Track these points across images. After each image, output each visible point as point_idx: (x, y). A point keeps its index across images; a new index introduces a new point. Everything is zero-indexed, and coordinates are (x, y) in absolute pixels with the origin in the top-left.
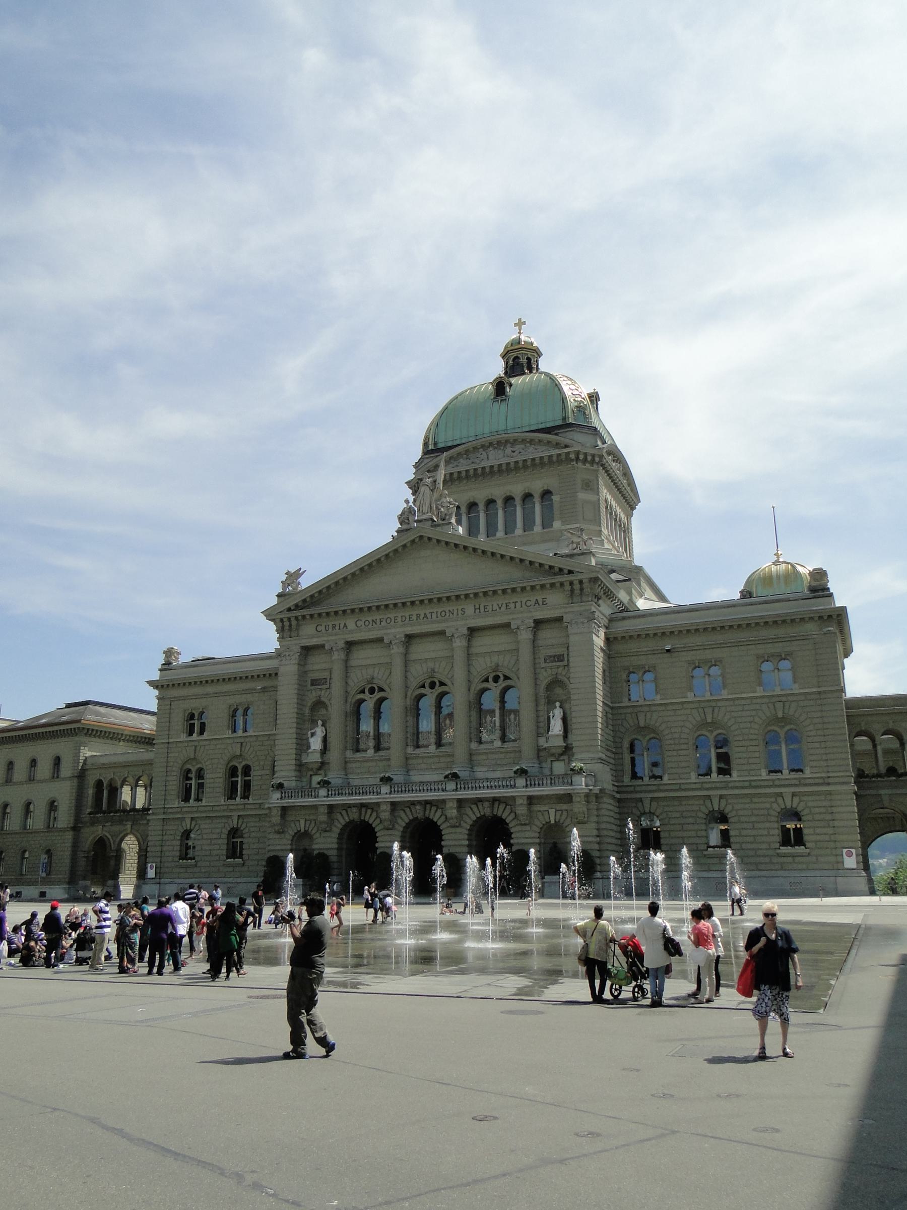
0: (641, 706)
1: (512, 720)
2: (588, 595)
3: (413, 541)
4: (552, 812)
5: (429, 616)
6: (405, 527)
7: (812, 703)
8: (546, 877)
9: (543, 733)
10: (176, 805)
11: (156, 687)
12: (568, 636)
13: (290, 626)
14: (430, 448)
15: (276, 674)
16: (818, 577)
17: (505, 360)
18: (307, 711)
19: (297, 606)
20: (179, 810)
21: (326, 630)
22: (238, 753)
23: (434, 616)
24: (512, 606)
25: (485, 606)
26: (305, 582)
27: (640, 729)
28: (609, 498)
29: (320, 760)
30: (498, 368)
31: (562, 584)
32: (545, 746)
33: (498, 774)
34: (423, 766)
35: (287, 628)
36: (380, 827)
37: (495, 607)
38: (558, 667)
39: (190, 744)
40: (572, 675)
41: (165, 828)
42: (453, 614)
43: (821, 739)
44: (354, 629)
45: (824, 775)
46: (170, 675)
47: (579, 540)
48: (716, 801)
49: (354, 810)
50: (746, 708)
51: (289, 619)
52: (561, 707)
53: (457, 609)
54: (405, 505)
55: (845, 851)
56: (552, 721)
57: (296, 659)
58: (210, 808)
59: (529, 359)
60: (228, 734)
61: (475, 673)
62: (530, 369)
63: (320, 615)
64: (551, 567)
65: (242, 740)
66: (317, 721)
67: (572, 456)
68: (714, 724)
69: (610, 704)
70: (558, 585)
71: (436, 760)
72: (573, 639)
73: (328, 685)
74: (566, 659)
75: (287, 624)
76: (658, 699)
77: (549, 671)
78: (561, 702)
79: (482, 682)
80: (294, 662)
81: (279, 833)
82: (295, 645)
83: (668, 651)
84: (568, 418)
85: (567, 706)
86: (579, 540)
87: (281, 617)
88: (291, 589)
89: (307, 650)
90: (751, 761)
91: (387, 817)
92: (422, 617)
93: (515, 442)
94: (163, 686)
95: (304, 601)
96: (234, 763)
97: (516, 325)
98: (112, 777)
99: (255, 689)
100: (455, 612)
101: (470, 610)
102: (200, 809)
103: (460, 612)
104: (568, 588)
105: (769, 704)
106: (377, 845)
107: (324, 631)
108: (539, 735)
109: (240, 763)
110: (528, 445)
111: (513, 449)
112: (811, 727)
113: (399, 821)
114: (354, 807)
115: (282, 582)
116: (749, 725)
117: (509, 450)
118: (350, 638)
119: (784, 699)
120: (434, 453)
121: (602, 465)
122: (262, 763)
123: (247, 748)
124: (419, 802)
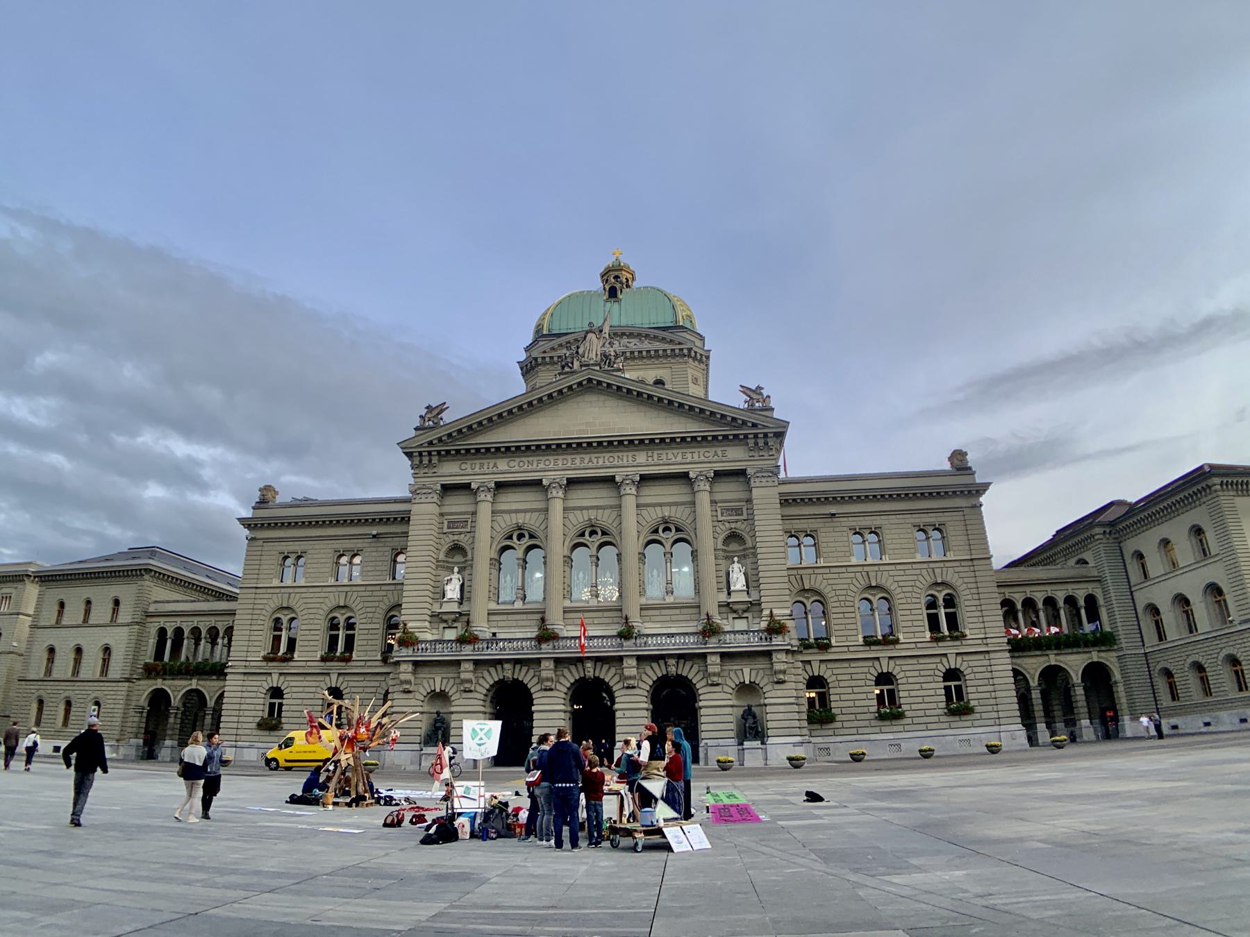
3: (580, 384)
4: (746, 671)
5: (595, 460)
7: (966, 569)
8: (745, 743)
11: (248, 527)
12: (751, 491)
13: (430, 461)
14: (545, 333)
17: (606, 277)
18: (442, 556)
19: (440, 440)
22: (342, 604)
24: (689, 456)
26: (447, 417)
27: (804, 590)
31: (746, 436)
32: (729, 601)
36: (538, 687)
37: (670, 456)
39: (283, 590)
42: (622, 460)
48: (884, 662)
49: (507, 666)
50: (907, 572)
51: (430, 453)
53: (627, 456)
58: (304, 664)
59: (626, 279)
61: (644, 523)
64: (734, 419)
67: (685, 351)
70: (742, 437)
71: (600, 614)
72: (756, 493)
73: (469, 526)
74: (745, 511)
76: (821, 563)
77: (727, 524)
78: (738, 557)
83: (834, 514)
88: (431, 423)
89: (447, 489)
91: (549, 676)
92: (586, 461)
95: (450, 435)
99: (370, 534)
100: (625, 459)
101: (641, 457)
103: (630, 459)
104: (751, 442)
106: (534, 708)
112: (967, 592)
113: (562, 680)
114: (506, 663)
115: (421, 417)
116: (910, 589)
119: (941, 565)
123: (353, 599)
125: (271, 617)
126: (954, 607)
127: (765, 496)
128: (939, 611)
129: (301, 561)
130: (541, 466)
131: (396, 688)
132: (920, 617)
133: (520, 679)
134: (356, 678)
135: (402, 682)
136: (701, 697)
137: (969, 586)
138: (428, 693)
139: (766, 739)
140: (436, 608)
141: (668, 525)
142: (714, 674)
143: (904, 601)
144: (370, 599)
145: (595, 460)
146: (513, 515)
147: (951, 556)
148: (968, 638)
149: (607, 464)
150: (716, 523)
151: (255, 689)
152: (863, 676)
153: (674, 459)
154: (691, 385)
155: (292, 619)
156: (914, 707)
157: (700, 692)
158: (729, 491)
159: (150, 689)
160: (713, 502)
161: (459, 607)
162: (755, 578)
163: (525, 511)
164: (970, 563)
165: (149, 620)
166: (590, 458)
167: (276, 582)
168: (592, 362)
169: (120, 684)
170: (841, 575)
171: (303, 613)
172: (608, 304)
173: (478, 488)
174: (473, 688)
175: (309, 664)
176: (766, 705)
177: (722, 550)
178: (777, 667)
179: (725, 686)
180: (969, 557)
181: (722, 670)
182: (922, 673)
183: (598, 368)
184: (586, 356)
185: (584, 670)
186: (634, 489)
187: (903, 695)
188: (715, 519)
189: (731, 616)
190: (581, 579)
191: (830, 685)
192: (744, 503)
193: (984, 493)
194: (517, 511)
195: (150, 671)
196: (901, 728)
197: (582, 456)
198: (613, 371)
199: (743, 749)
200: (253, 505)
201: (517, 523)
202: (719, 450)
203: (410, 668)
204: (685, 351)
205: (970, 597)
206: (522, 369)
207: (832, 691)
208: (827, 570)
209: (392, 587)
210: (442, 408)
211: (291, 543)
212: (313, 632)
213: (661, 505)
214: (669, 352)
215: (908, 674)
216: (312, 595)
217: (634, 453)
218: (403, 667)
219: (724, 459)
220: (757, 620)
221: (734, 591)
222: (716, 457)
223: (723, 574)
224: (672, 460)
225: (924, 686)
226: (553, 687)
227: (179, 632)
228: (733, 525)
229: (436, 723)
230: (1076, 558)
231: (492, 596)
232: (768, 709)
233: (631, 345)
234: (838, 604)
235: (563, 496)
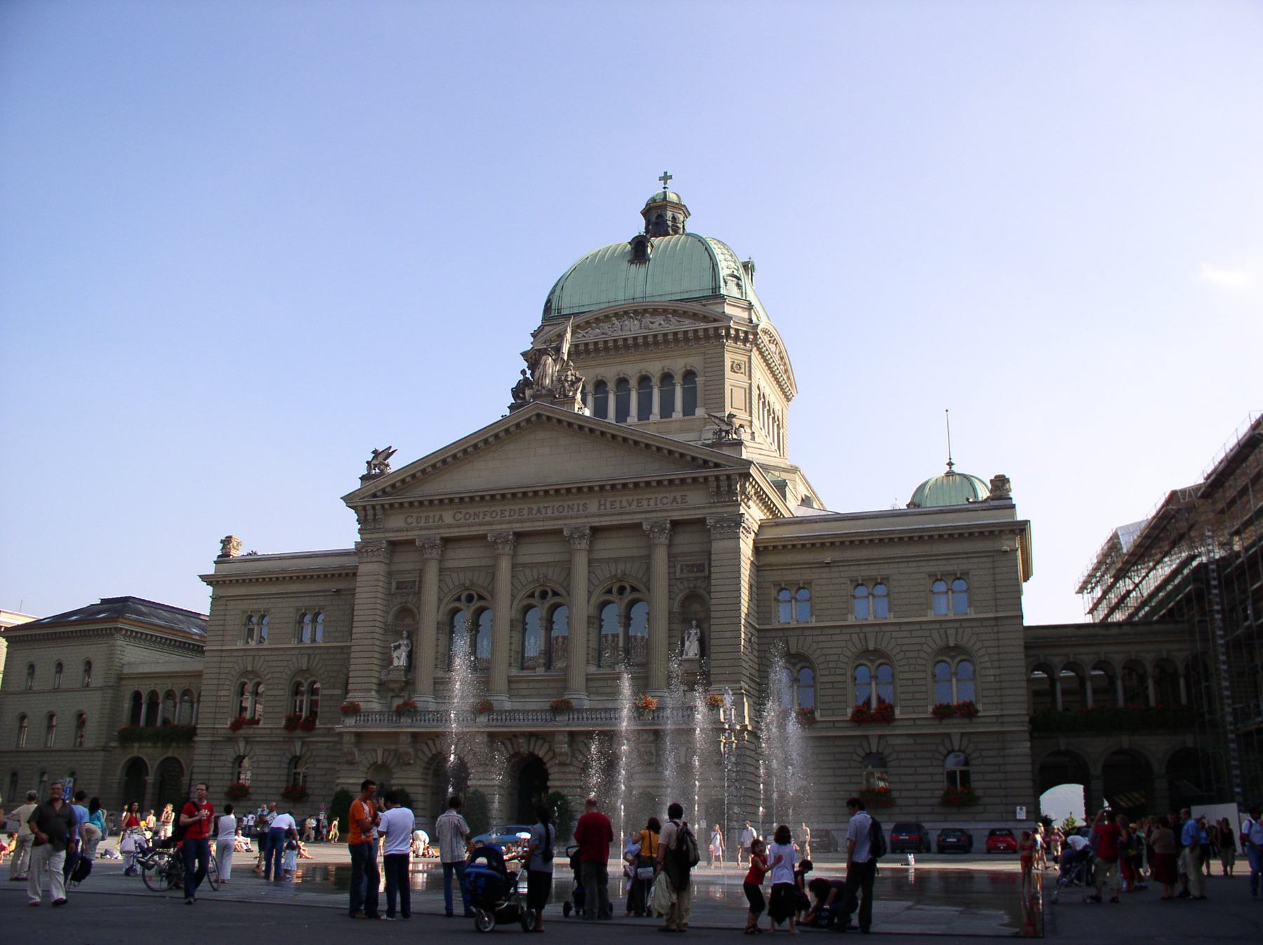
0: (793, 629)
3: (528, 420)
5: (543, 511)
11: (210, 583)
12: (711, 542)
13: (375, 515)
15: (355, 574)
16: (999, 484)
19: (384, 491)
23: (549, 511)
24: (645, 503)
25: (611, 502)
26: (395, 464)
28: (763, 384)
30: (638, 226)
31: (706, 479)
35: (370, 517)
37: (624, 504)
40: (713, 589)
42: (572, 509)
43: (998, 672)
44: (451, 521)
45: (997, 713)
46: (226, 568)
47: (728, 428)
48: (874, 742)
50: (915, 634)
51: (374, 507)
52: (698, 626)
53: (578, 504)
54: (521, 377)
56: (687, 643)
58: (269, 731)
59: (674, 218)
60: (294, 643)
61: (596, 582)
62: (676, 232)
63: (411, 504)
64: (694, 458)
65: (310, 652)
68: (878, 653)
69: (757, 626)
70: (701, 480)
75: (370, 512)
76: (813, 622)
77: (685, 583)
81: (351, 763)
85: (705, 626)
86: (728, 428)
88: (377, 471)
90: (917, 696)
92: (534, 512)
93: (655, 312)
94: (218, 582)
95: (393, 486)
96: (299, 679)
97: (660, 179)
100: (575, 508)
101: (593, 506)
103: (581, 507)
107: (414, 524)
109: (306, 679)
111: (653, 320)
112: (986, 658)
115: (368, 462)
117: (647, 319)
118: (446, 533)
119: (957, 625)
121: (757, 345)
124: (523, 734)
130: (488, 518)
137: (990, 651)
138: (372, 765)
141: (624, 584)
143: (906, 668)
146: (461, 575)
148: (980, 714)
149: (556, 514)
153: (628, 509)
155: (258, 684)
156: (904, 794)
158: (688, 542)
160: (672, 557)
161: (406, 676)
164: (993, 623)
165: (124, 682)
167: (240, 645)
168: (544, 392)
169: (96, 754)
170: (834, 638)
172: (633, 266)
174: (412, 762)
180: (991, 615)
188: (672, 576)
190: (532, 645)
195: (127, 737)
197: (530, 506)
200: (216, 559)
201: (464, 584)
202: (678, 495)
205: (989, 664)
210: (388, 453)
213: (616, 560)
217: (586, 501)
219: (684, 506)
222: (674, 504)
224: (626, 509)
225: (920, 770)
227: (153, 695)
231: (439, 663)
233: (654, 326)
235: (511, 552)
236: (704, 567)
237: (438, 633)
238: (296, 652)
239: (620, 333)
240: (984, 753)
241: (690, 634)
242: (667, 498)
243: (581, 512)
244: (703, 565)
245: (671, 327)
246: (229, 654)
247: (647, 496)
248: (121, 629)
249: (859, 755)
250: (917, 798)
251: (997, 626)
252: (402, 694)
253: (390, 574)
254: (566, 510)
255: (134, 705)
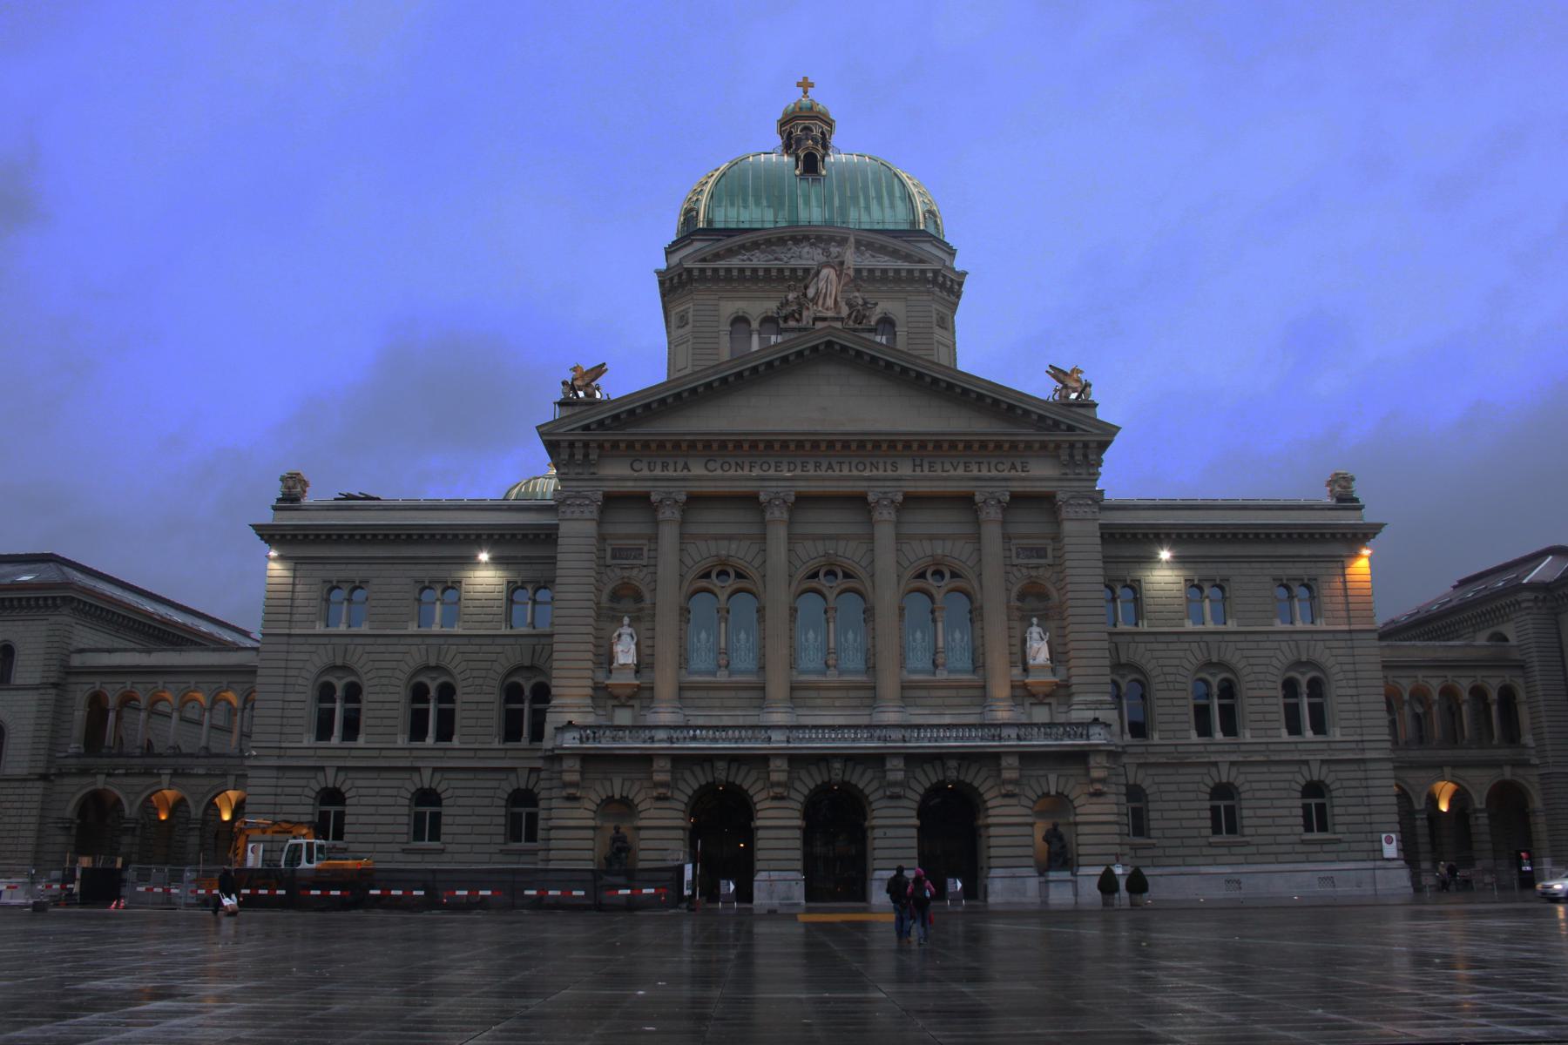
1: (957, 641)
2: (1093, 465)
3: (815, 349)
4: (1052, 778)
5: (837, 467)
6: (792, 323)
7: (1342, 644)
9: (1016, 663)
10: (305, 744)
12: (1058, 522)
13: (586, 456)
14: (701, 226)
18: (605, 602)
19: (601, 423)
20: (311, 752)
21: (651, 471)
25: (930, 463)
26: (612, 388)
29: (638, 682)
31: (1058, 446)
32: (1027, 681)
33: (947, 720)
34: (819, 702)
35: (579, 456)
37: (948, 466)
38: (1037, 567)
41: (282, 782)
44: (702, 474)
49: (721, 765)
50: (1262, 645)
51: (586, 445)
52: (1038, 625)
53: (885, 463)
55: (1384, 836)
57: (591, 512)
59: (822, 133)
61: (906, 564)
63: (646, 445)
64: (1042, 418)
66: (620, 620)
67: (930, 275)
68: (1222, 665)
70: (1052, 446)
72: (1068, 527)
73: (646, 560)
77: (1024, 571)
79: (914, 578)
80: (587, 515)
82: (596, 491)
84: (919, 223)
87: (571, 438)
89: (612, 501)
92: (824, 467)
95: (616, 417)
97: (799, 85)
98: (97, 688)
100: (881, 466)
101: (905, 469)
102: (354, 753)
105: (1290, 643)
106: (759, 823)
108: (1013, 664)
110: (863, 248)
115: (564, 383)
118: (696, 487)
119: (1308, 636)
120: (712, 235)
122: (480, 681)
124: (835, 756)
125: (316, 680)
126: (1320, 695)
127: (1080, 532)
128: (1302, 701)
129: (358, 595)
131: (555, 793)
132: (1274, 709)
133: (738, 782)
134: (461, 776)
135: (566, 785)
136: (991, 812)
137: (1346, 667)
139: (1075, 868)
140: (601, 676)
141: (940, 568)
142: (1010, 782)
144: (474, 657)
145: (837, 467)
147: (1321, 625)
149: (855, 473)
150: (1009, 568)
151: (299, 791)
152: (1190, 787)
153: (952, 472)
154: (937, 330)
157: (989, 804)
158: (1030, 525)
159: (84, 791)
160: (1007, 538)
162: (1060, 649)
163: (730, 538)
164: (1347, 636)
166: (830, 463)
168: (830, 314)
169: (29, 784)
170: (1172, 646)
171: (370, 675)
173: (661, 501)
174: (669, 794)
175: (384, 753)
176: (1076, 824)
177: (1018, 609)
178: (1095, 774)
179: (1023, 798)
181: (1021, 776)
182: (1274, 785)
183: (838, 325)
184: (820, 302)
185: (829, 772)
186: (893, 512)
187: (1246, 814)
189: (1028, 702)
191: (1150, 798)
192: (1049, 541)
193: (1374, 537)
194: (717, 538)
196: (1242, 859)
198: (863, 330)
199: (1047, 882)
200: (274, 504)
203: (577, 765)
204: (930, 275)
206: (662, 283)
207: (1151, 806)
208: (1152, 638)
209: (512, 641)
210: (599, 370)
211: (343, 567)
212: (387, 706)
214: (904, 274)
215: (1255, 785)
216: (382, 649)
218: (567, 764)
220: (1063, 709)
221: (1033, 666)
223: (1017, 641)
224: (950, 477)
226: (786, 794)
228: (1034, 573)
229: (614, 842)
230: (1488, 632)
232: (1081, 829)
234: (1165, 686)
236: (1046, 552)
237: (681, 621)
238: (419, 641)
239: (800, 262)
240: (1346, 784)
241: (1031, 633)
242: (1003, 463)
243: (889, 473)
244: (1045, 550)
245: (866, 262)
246: (301, 640)
247: (980, 460)
248: (73, 599)
249: (1207, 785)
250: (1275, 835)
251: (1351, 640)
252: (630, 703)
253: (602, 538)
254: (868, 469)
255: (89, 713)
